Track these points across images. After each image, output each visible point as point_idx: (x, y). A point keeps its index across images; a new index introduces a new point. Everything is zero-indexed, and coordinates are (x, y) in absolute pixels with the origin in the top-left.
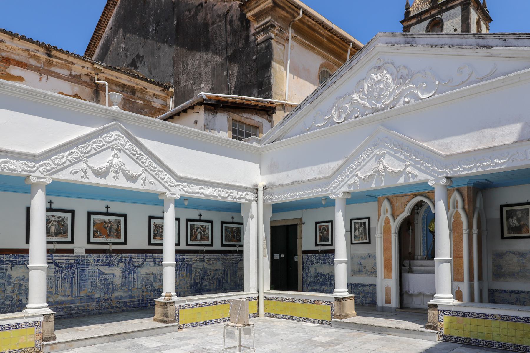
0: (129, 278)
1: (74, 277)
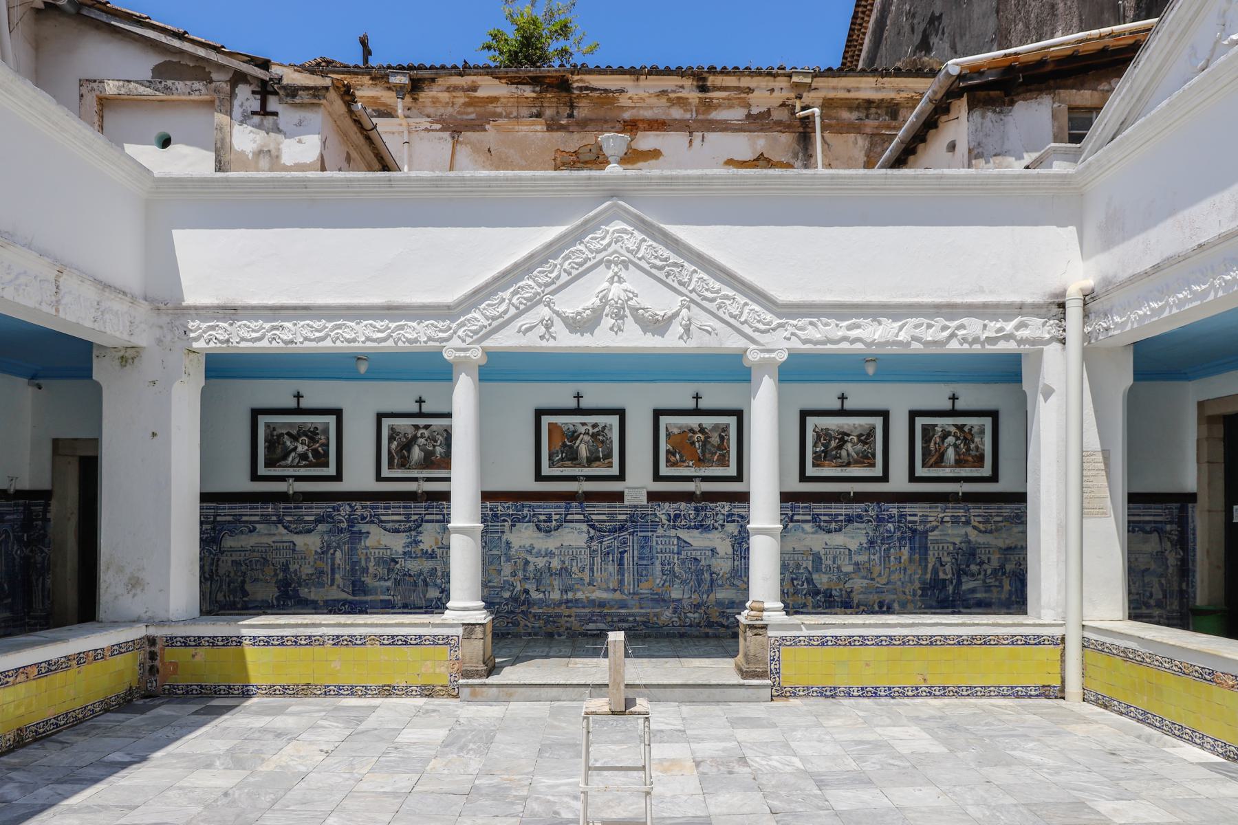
1: (626, 551)
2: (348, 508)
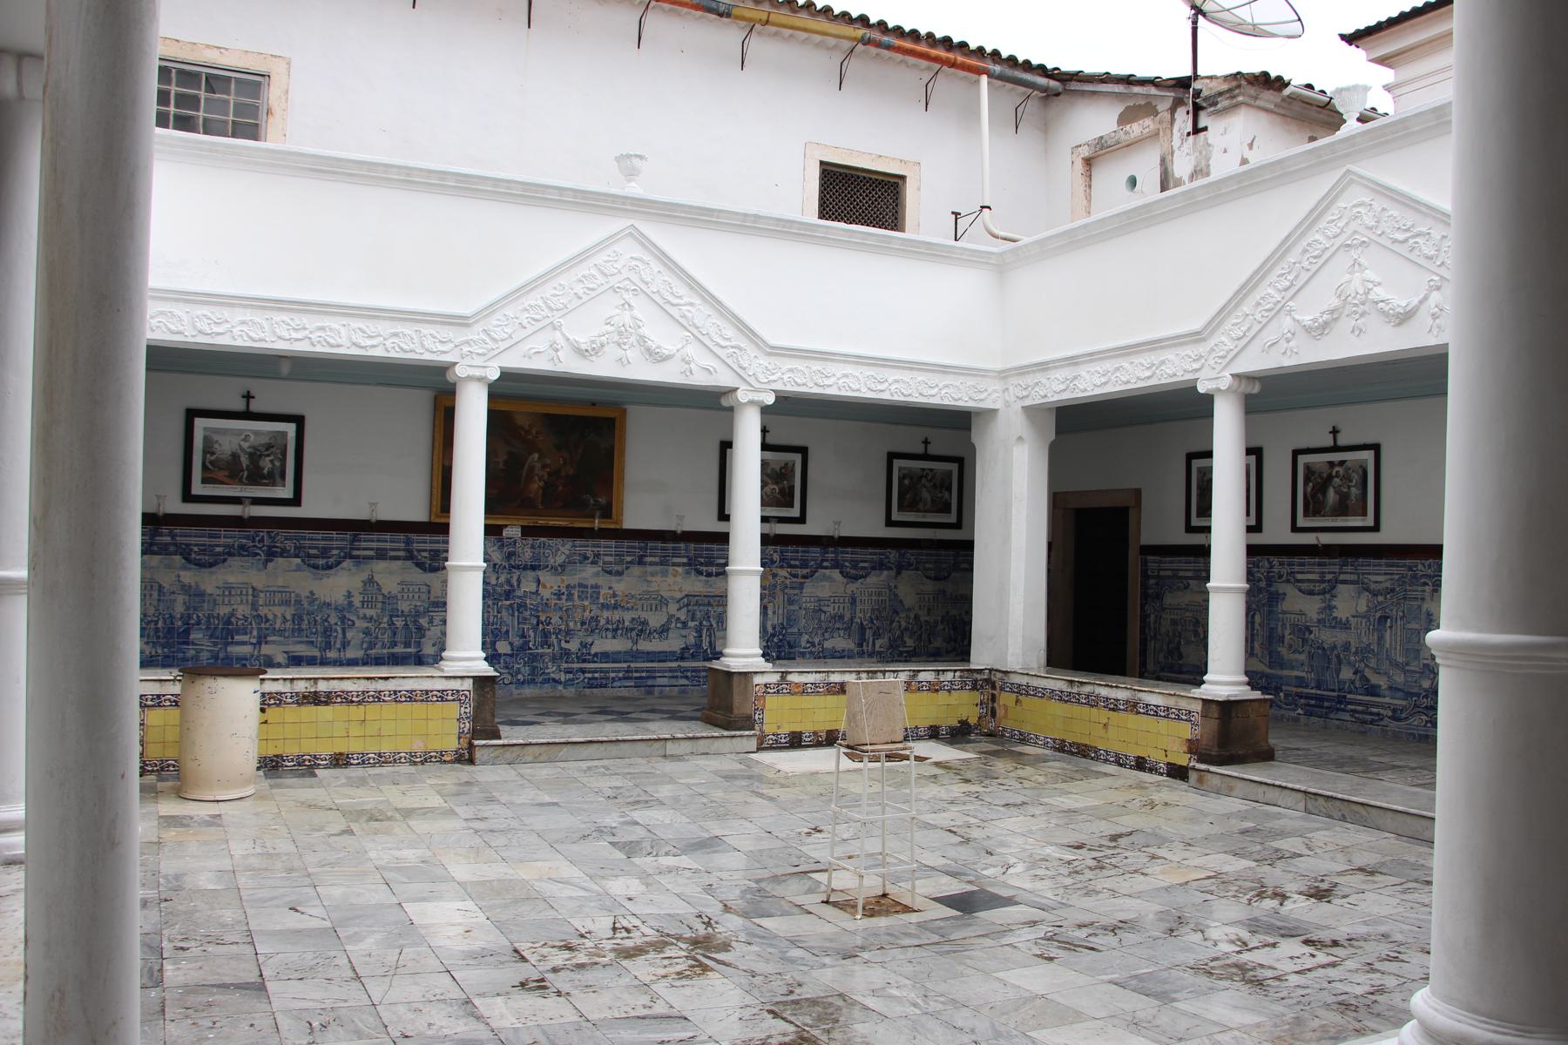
2: (1266, 564)
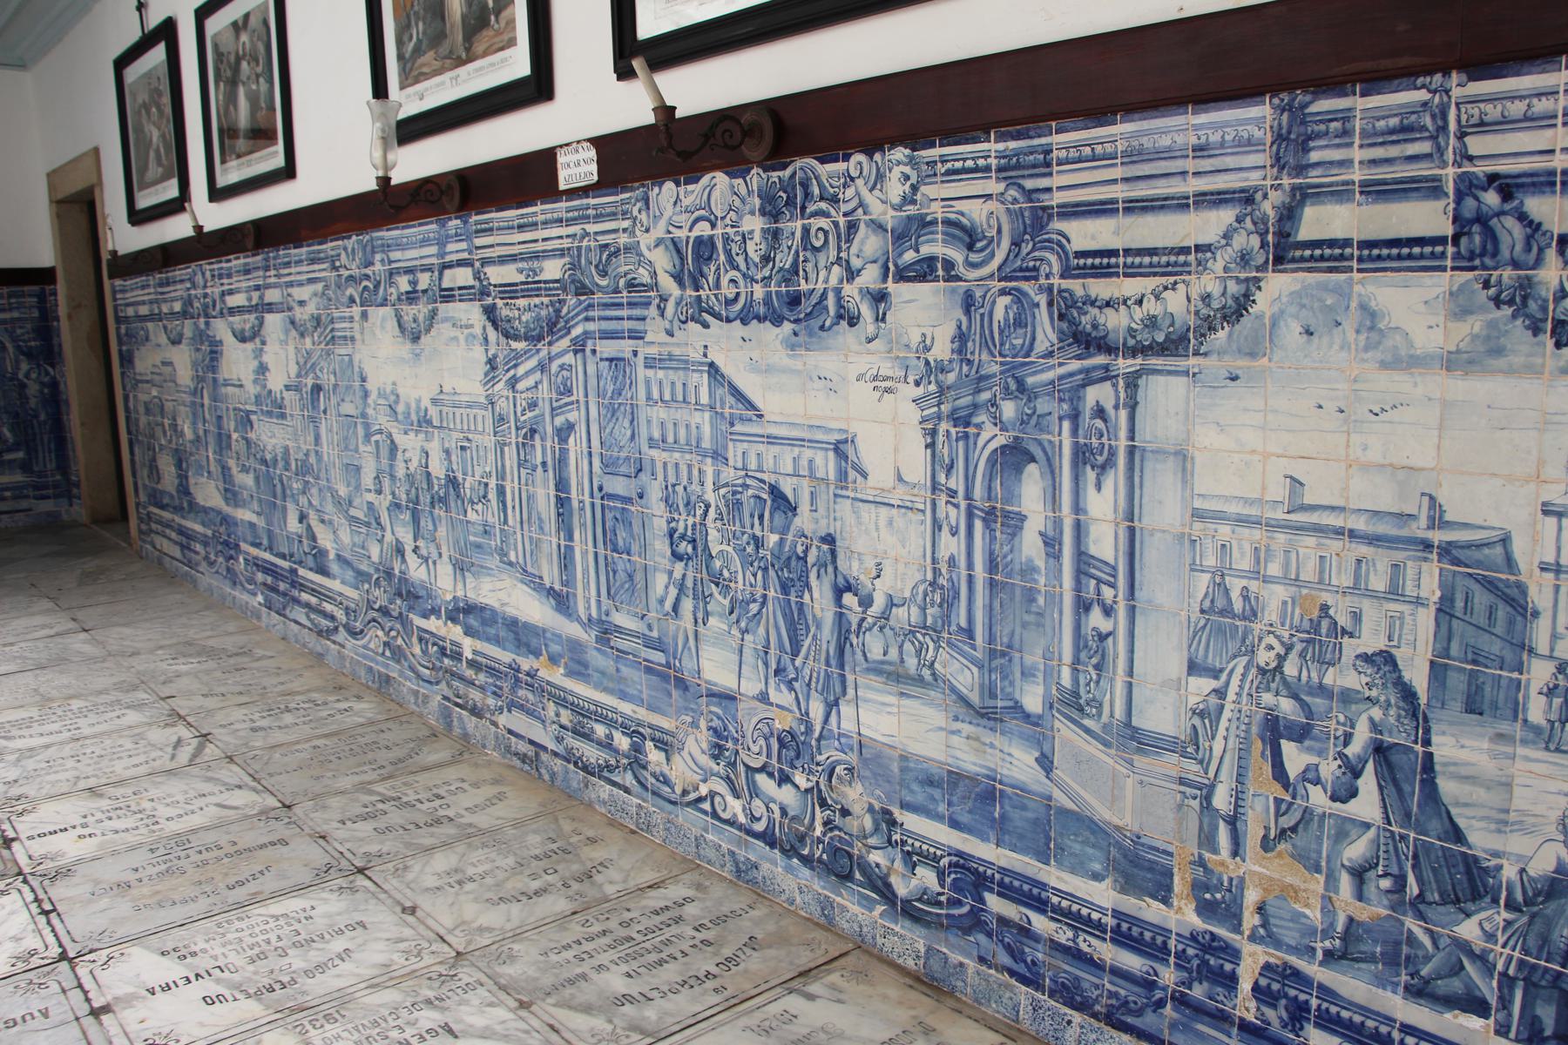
0: (1015, 522)
